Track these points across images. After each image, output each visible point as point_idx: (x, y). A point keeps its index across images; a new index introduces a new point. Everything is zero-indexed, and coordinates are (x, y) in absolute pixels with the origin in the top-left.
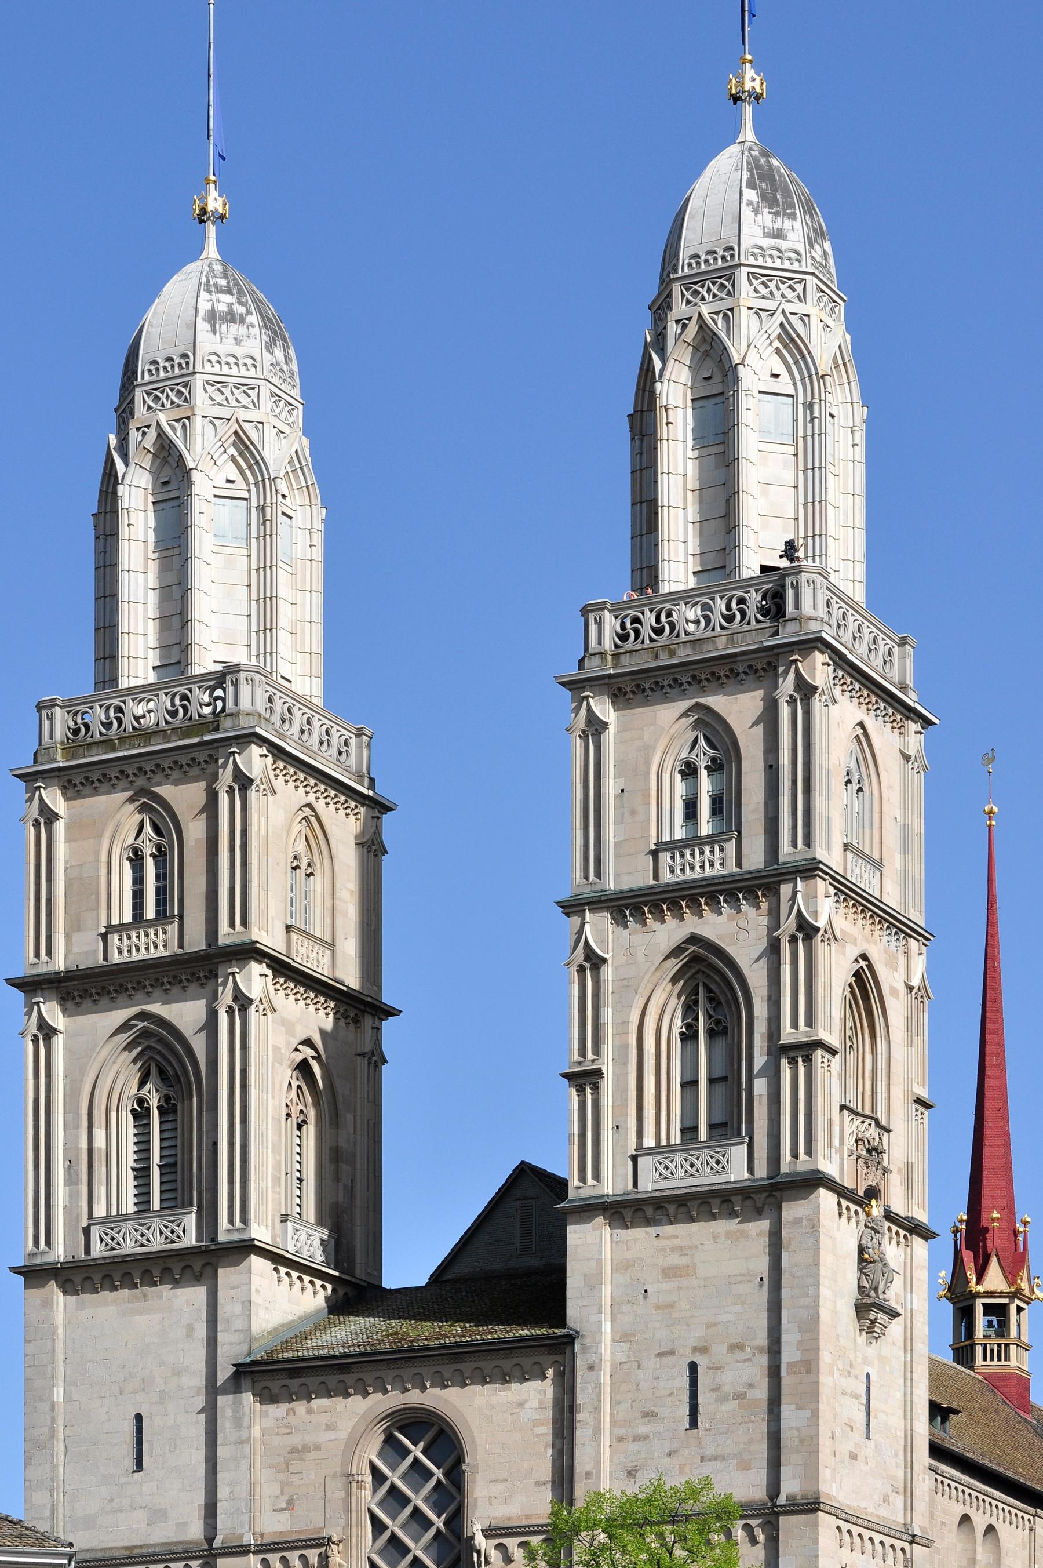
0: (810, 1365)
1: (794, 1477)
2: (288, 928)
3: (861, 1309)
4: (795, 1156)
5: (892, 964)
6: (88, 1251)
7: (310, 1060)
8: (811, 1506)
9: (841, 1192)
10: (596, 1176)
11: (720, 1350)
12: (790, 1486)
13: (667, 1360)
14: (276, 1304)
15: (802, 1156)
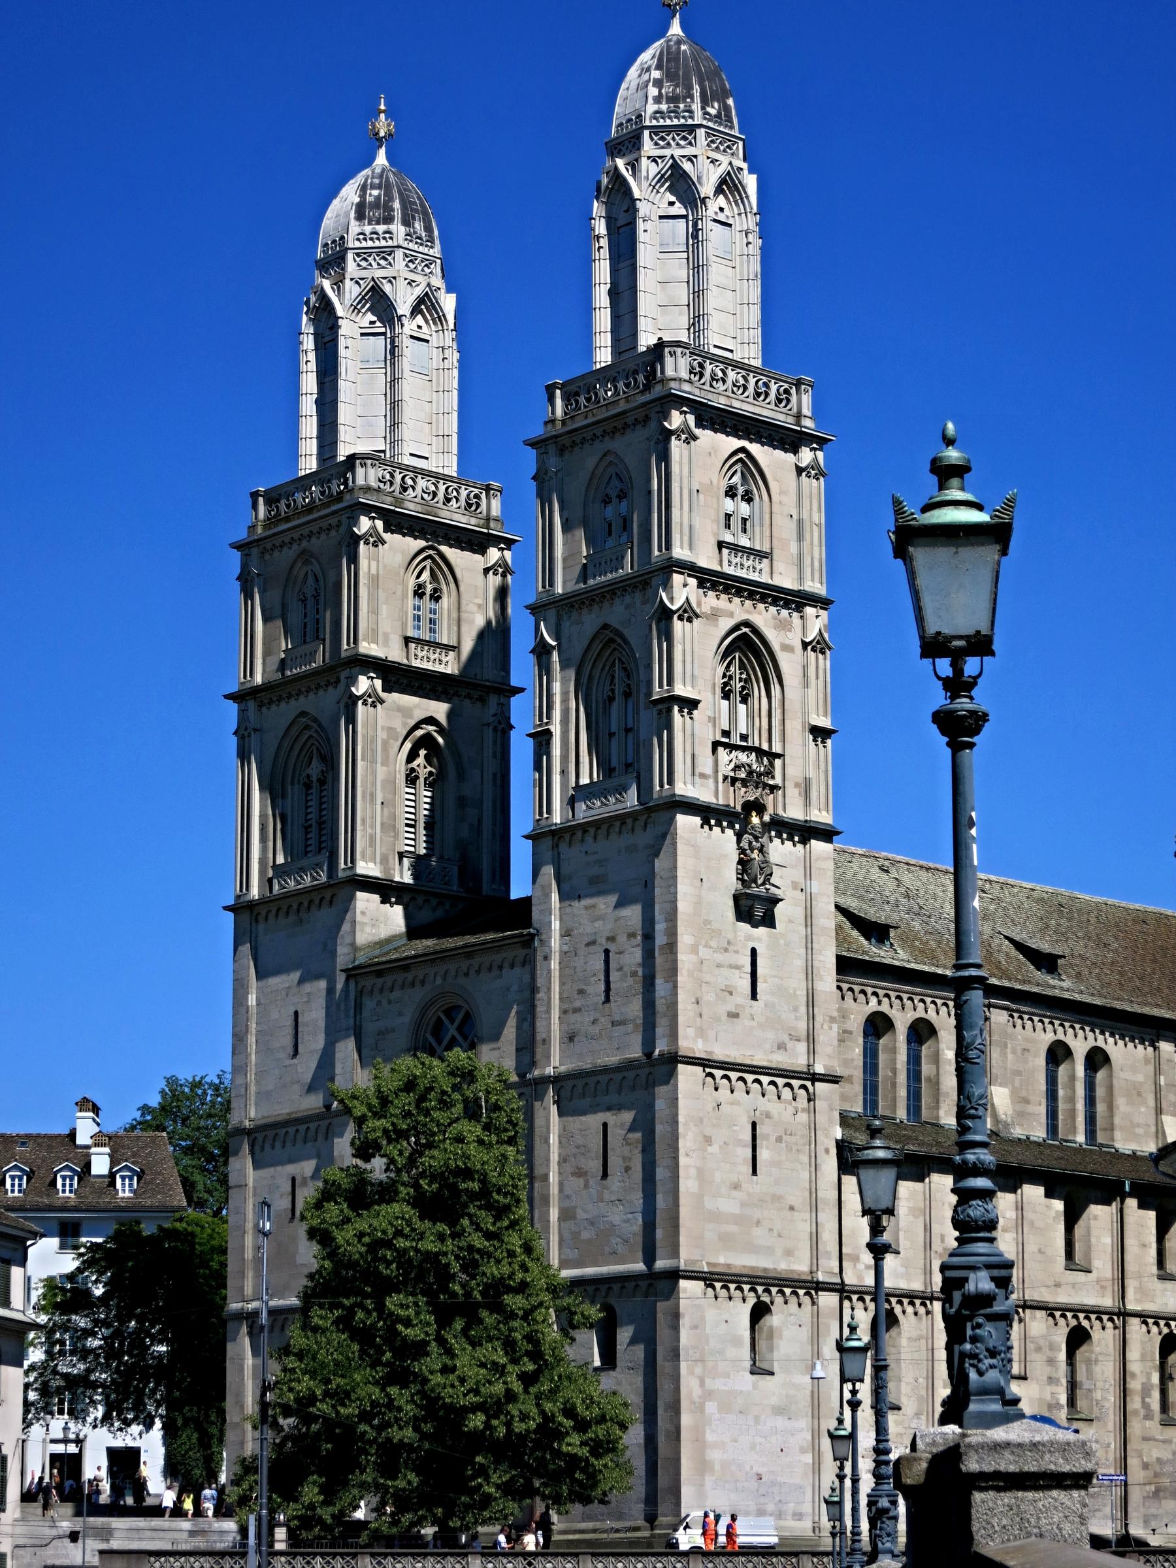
0: (672, 947)
1: (664, 1036)
2: (407, 640)
3: (736, 898)
4: (662, 786)
5: (784, 626)
6: (271, 891)
7: (435, 734)
8: (673, 1059)
10: (549, 811)
11: (622, 939)
12: (661, 1047)
13: (592, 948)
14: (378, 922)
15: (666, 786)
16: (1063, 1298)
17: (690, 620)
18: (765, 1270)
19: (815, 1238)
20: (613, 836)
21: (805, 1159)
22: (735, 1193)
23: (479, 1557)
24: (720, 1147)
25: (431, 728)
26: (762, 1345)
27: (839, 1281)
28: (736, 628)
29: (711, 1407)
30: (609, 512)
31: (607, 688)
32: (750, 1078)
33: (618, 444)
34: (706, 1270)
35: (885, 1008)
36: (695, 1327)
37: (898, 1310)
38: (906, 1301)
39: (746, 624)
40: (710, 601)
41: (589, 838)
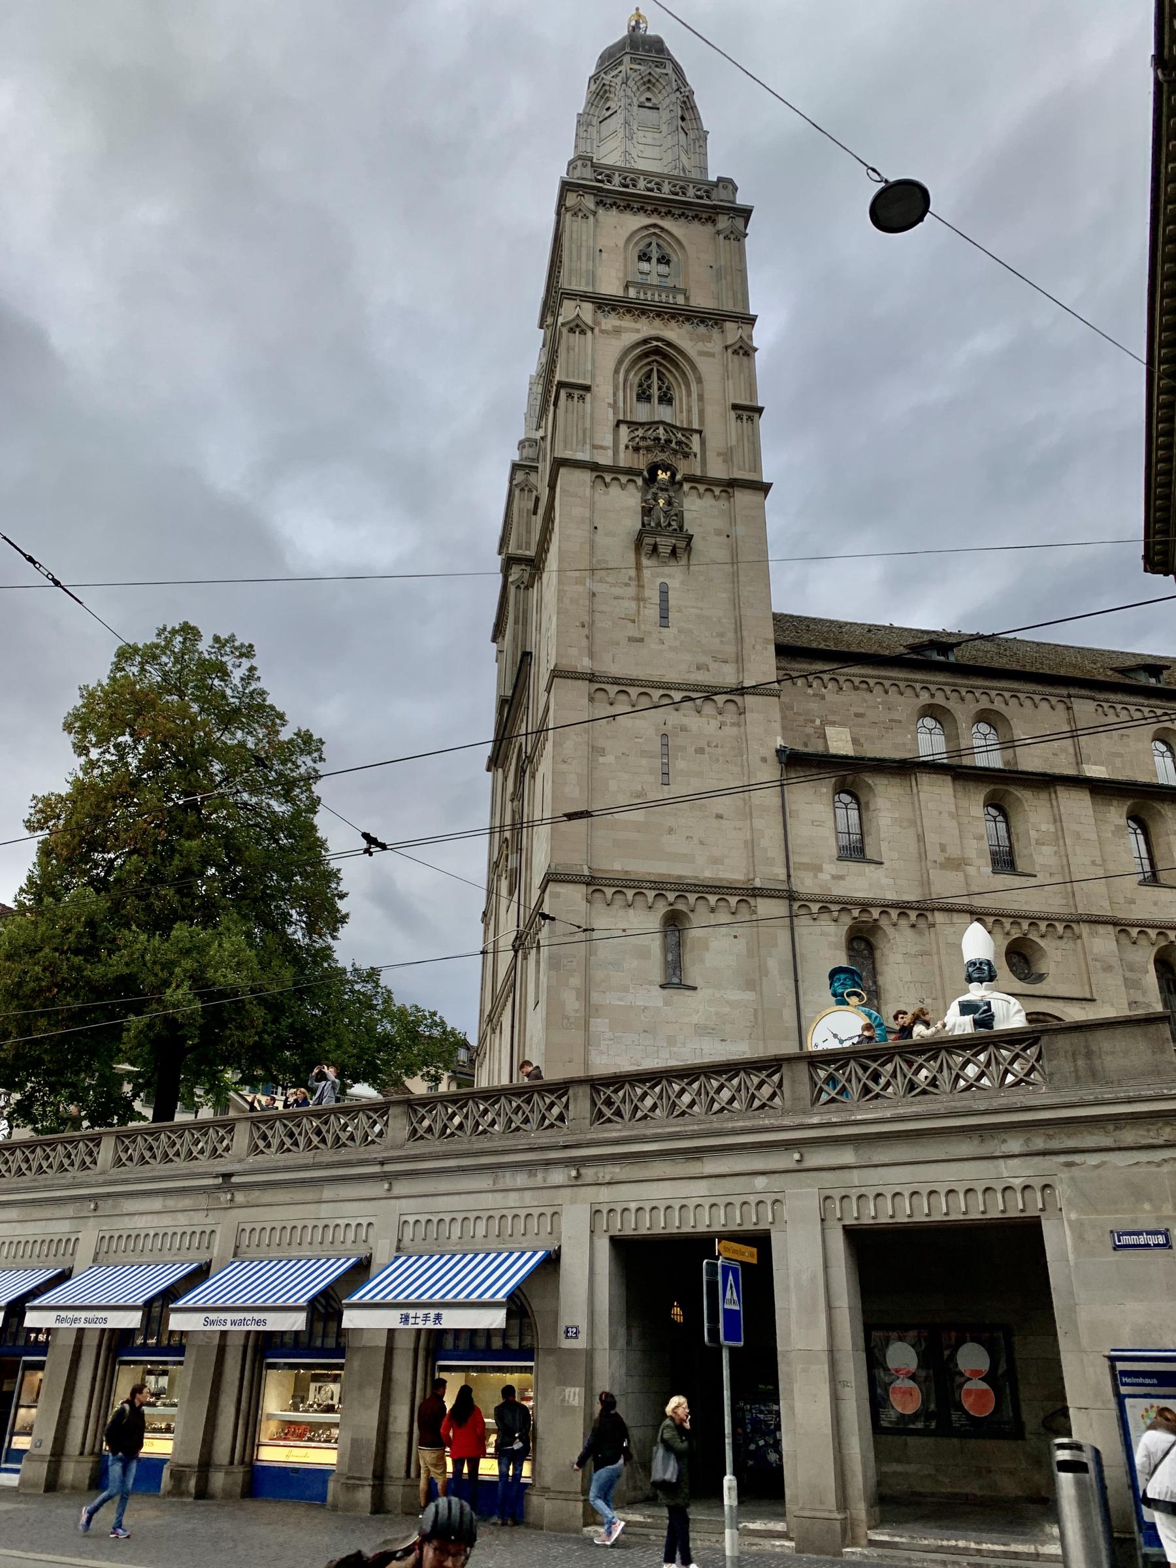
9: (594, 467)
16: (1138, 913)
17: (583, 332)
18: (680, 877)
19: (751, 846)
24: (616, 757)
27: (785, 887)
28: (645, 341)
29: (599, 1025)
34: (586, 873)
35: (939, 699)
37: (884, 922)
38: (894, 913)
39: (658, 339)
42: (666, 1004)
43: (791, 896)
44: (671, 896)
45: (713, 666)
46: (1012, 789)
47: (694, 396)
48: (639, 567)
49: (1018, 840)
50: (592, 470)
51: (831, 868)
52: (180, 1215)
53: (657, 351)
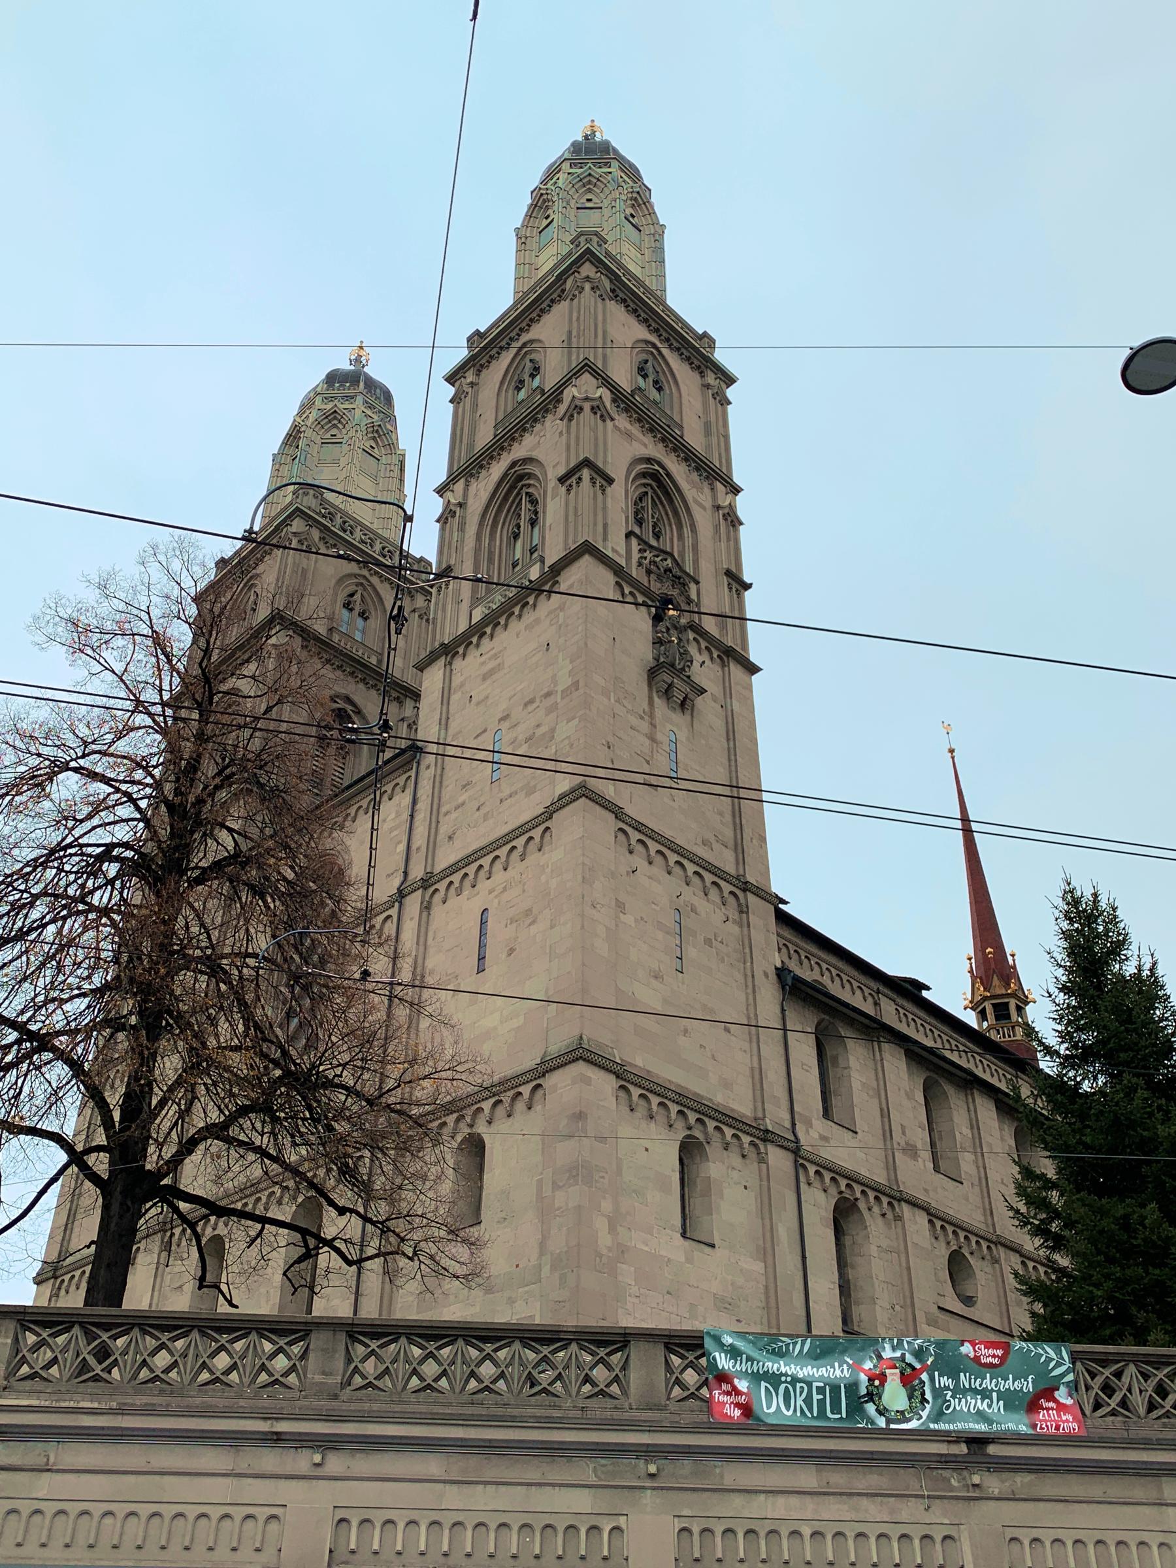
9: (618, 571)
18: (695, 1094)
19: (758, 1076)
20: (514, 624)
21: (740, 978)
22: (654, 982)
23: (11, 1325)
25: (349, 708)
26: (696, 1204)
29: (627, 1273)
30: (522, 395)
31: (514, 523)
32: (673, 858)
33: (535, 332)
36: (602, 1139)
37: (862, 1205)
40: (622, 421)
41: (485, 641)
42: (689, 1260)
43: (795, 1150)
44: (692, 1117)
45: (715, 846)
46: (942, 1082)
47: (688, 541)
48: (651, 703)
49: (941, 1138)
50: (616, 573)
51: (820, 1126)
52: (864, 1502)
53: (655, 476)
